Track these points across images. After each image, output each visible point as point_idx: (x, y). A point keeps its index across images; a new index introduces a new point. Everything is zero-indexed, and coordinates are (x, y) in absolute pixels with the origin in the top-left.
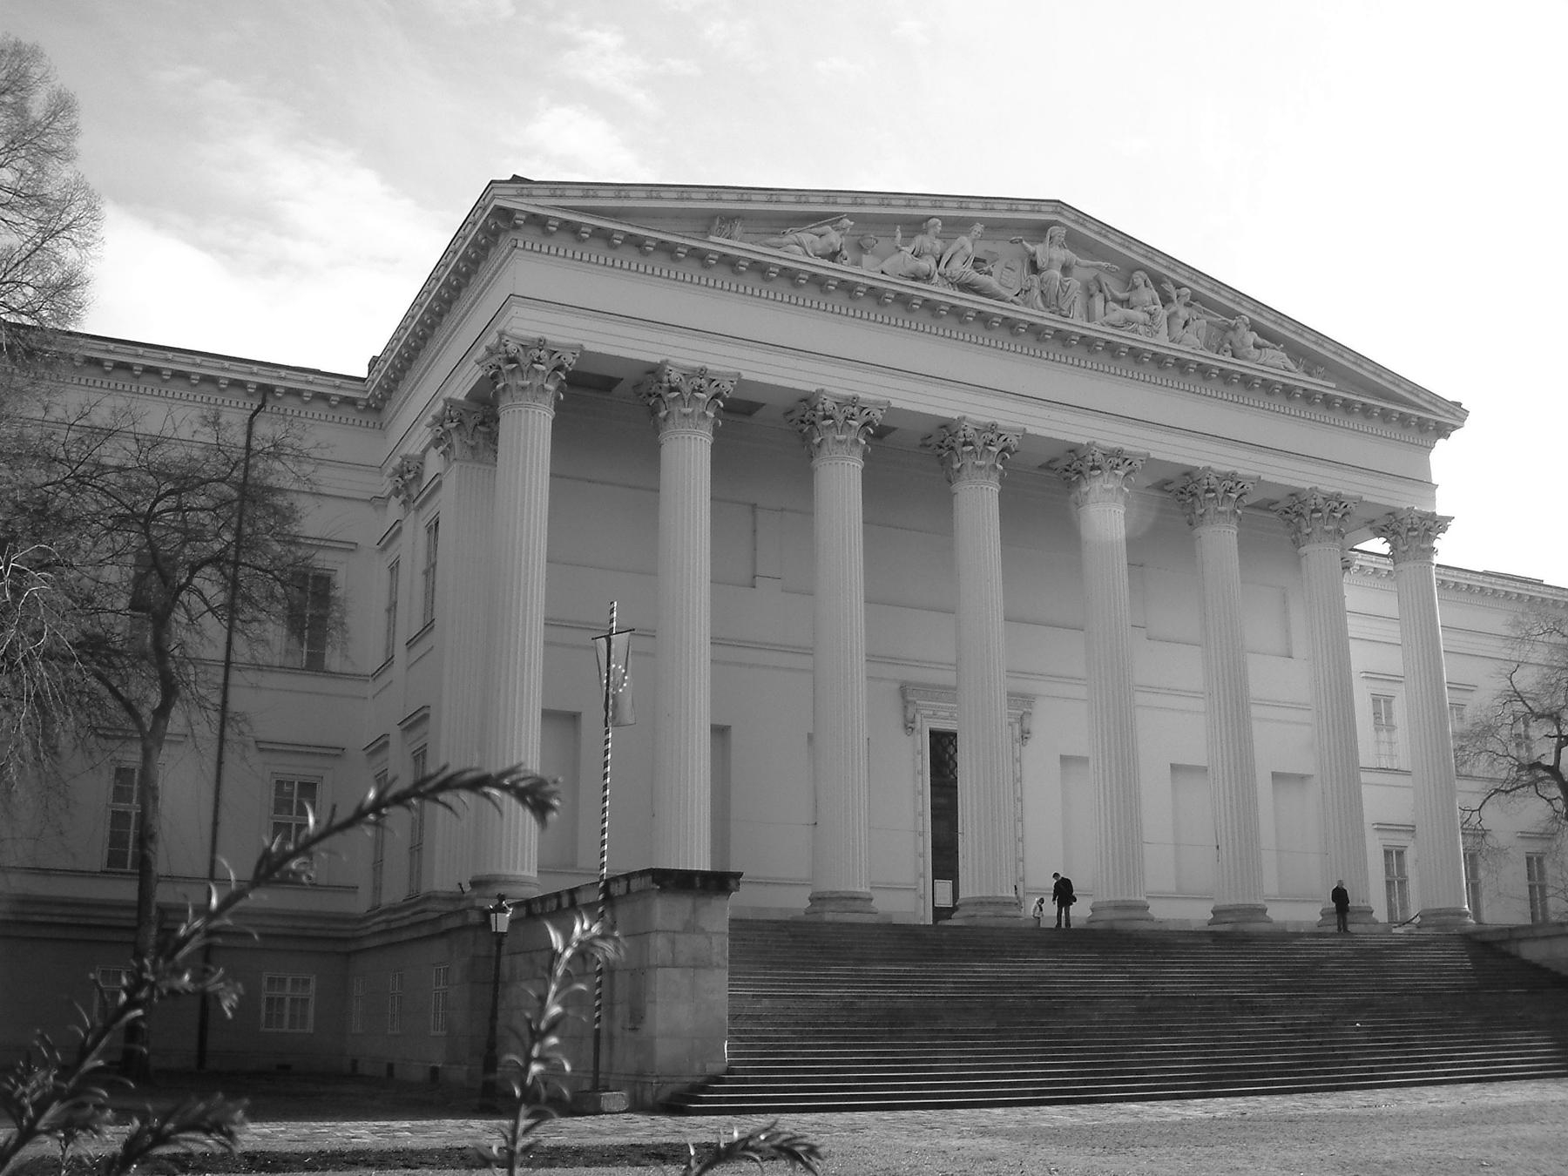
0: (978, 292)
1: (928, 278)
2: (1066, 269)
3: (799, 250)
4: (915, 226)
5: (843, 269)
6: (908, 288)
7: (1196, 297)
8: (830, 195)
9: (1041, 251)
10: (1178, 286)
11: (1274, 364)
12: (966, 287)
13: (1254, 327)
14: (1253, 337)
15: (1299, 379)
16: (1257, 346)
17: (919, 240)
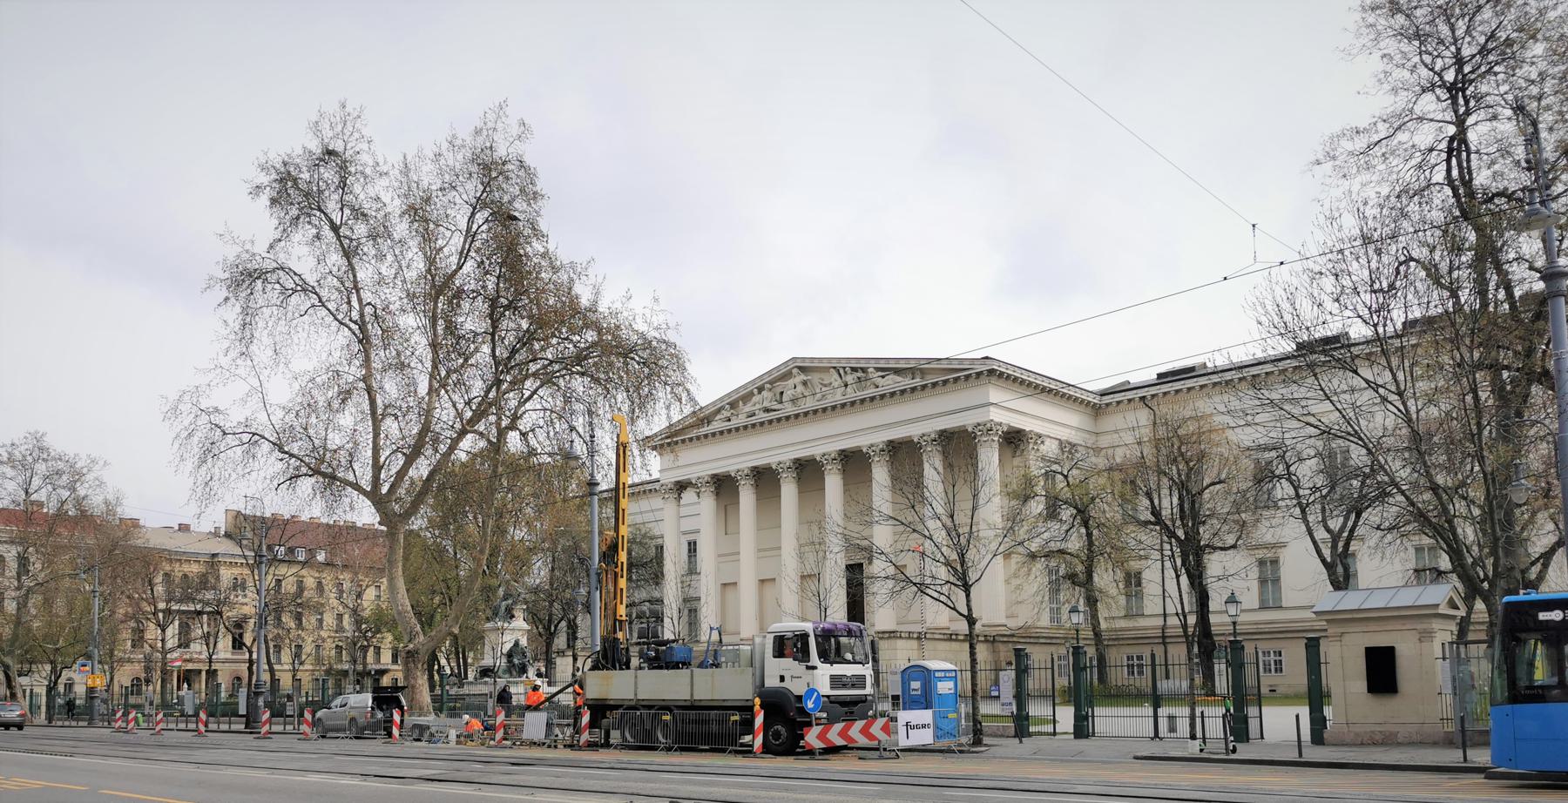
0: (775, 410)
1: (754, 415)
2: (805, 383)
3: (717, 425)
4: (751, 394)
5: (735, 422)
6: (753, 420)
7: (854, 370)
8: (721, 399)
9: (791, 382)
10: (844, 368)
11: (891, 383)
12: (767, 410)
13: (878, 369)
14: (875, 375)
15: (906, 382)
16: (883, 377)
17: (754, 399)
